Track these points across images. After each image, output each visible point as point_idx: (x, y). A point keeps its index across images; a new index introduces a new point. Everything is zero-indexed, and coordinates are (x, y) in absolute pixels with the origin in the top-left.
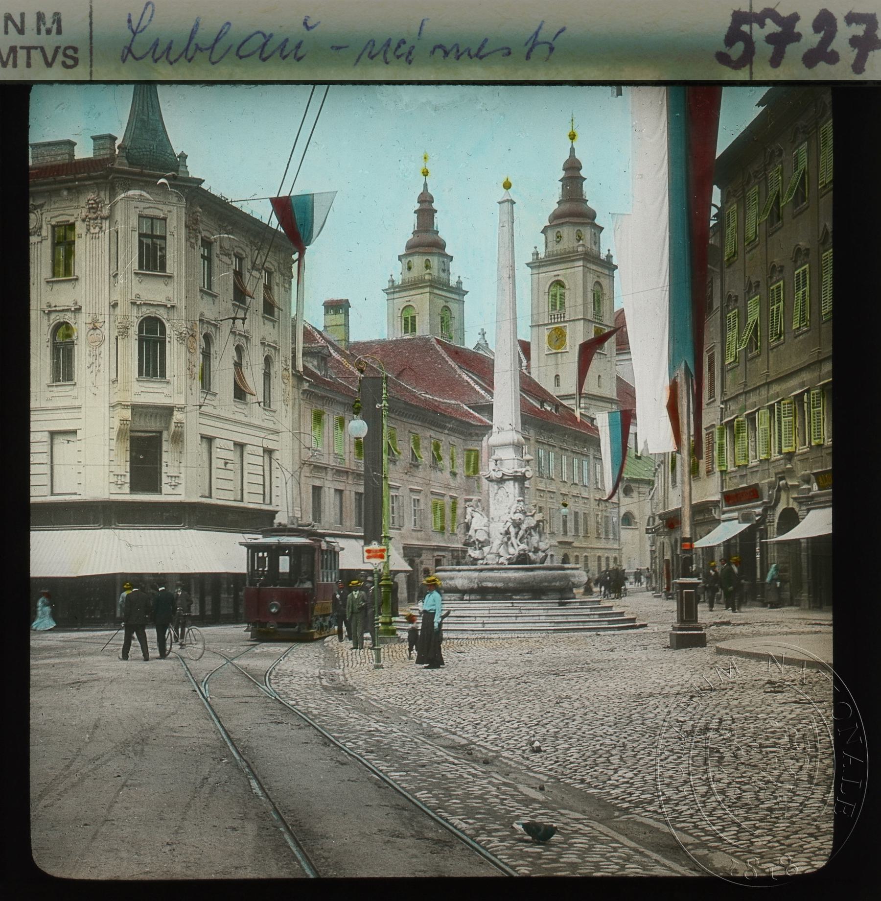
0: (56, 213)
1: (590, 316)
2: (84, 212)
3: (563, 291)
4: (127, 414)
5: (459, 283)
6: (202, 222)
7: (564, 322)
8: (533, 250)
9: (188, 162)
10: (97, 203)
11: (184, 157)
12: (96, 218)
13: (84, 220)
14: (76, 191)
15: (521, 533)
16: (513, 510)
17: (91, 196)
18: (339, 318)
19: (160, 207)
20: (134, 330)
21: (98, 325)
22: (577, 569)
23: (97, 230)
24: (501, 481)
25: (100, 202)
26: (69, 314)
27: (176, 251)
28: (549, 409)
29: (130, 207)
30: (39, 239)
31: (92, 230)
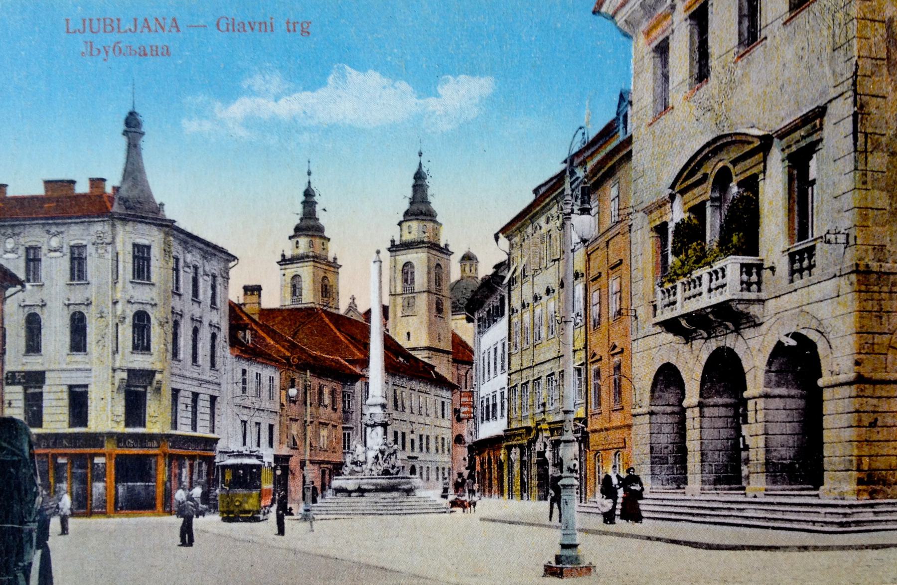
1: (433, 290)
4: (125, 375)
5: (335, 259)
8: (391, 238)
9: (165, 208)
11: (162, 205)
13: (93, 244)
20: (129, 320)
21: (104, 315)
23: (103, 251)
24: (374, 426)
26: (83, 307)
27: (158, 267)
29: (127, 237)
30: (61, 254)
31: (100, 251)
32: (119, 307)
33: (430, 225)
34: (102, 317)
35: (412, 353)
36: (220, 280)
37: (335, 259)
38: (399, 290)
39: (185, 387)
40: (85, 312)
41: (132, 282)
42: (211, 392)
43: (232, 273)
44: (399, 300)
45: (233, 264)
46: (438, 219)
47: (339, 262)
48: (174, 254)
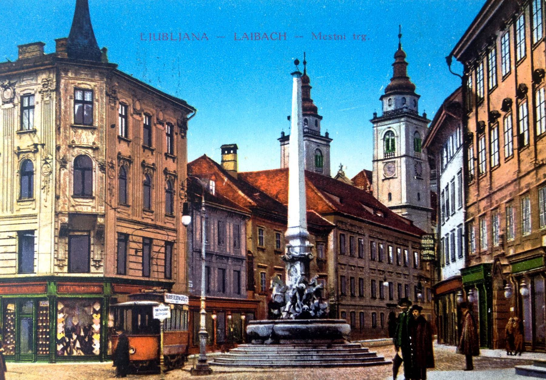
0: (24, 88)
3: (393, 138)
4: (66, 220)
5: (327, 134)
6: (119, 92)
7: (395, 158)
10: (48, 81)
12: (47, 91)
13: (40, 92)
14: (35, 73)
15: (304, 297)
16: (298, 281)
17: (44, 76)
18: (229, 157)
19: (88, 83)
20: (70, 165)
21: (48, 161)
22: (344, 322)
23: (48, 99)
25: (50, 80)
28: (379, 215)
31: (45, 99)
33: (408, 98)
34: (46, 163)
35: (394, 211)
36: (176, 129)
37: (327, 134)
38: (381, 156)
39: (159, 237)
40: (33, 159)
41: (72, 127)
42: (165, 238)
43: (190, 123)
44: (381, 165)
45: (191, 114)
46: (417, 92)
47: (330, 136)
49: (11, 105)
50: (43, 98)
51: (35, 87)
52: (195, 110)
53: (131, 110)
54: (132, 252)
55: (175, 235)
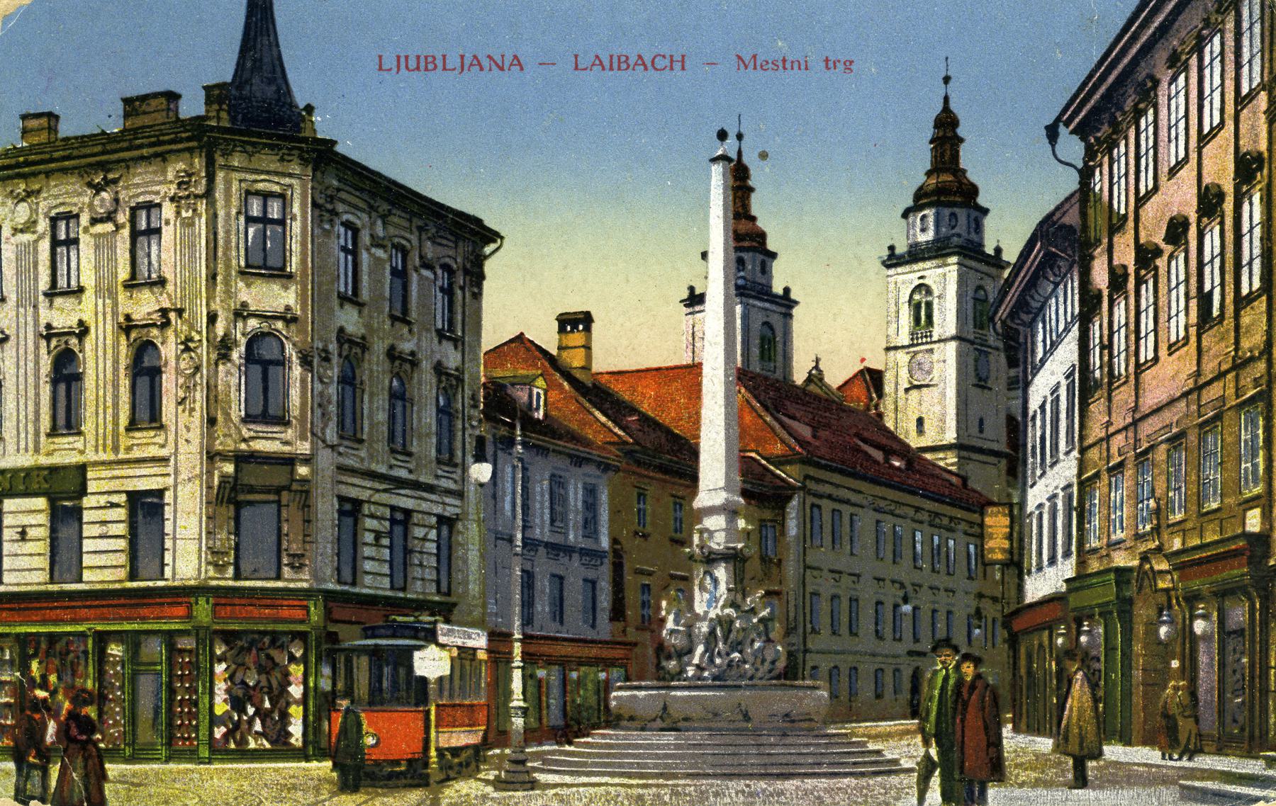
2: (173, 189)
3: (929, 299)
4: (229, 468)
5: (787, 290)
7: (932, 342)
10: (190, 175)
11: (309, 109)
12: (188, 197)
13: (172, 199)
18: (577, 338)
21: (192, 345)
23: (190, 213)
25: (193, 174)
28: (897, 464)
31: (184, 214)
32: (220, 329)
33: (962, 213)
34: (187, 349)
35: (928, 456)
37: (787, 290)
38: (904, 339)
39: (425, 506)
40: (158, 342)
41: (242, 273)
42: (438, 510)
43: (489, 267)
44: (902, 357)
45: (492, 246)
46: (982, 200)
47: (793, 296)
48: (345, 217)
49: (109, 227)
50: (178, 213)
51: (163, 189)
52: (502, 238)
53: (365, 238)
54: (369, 538)
55: (457, 502)
